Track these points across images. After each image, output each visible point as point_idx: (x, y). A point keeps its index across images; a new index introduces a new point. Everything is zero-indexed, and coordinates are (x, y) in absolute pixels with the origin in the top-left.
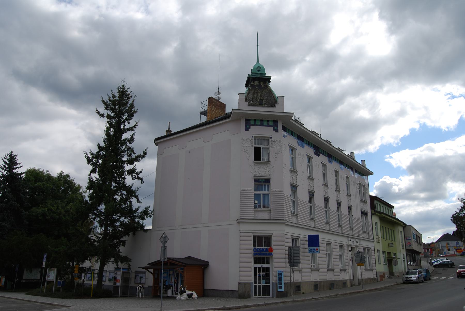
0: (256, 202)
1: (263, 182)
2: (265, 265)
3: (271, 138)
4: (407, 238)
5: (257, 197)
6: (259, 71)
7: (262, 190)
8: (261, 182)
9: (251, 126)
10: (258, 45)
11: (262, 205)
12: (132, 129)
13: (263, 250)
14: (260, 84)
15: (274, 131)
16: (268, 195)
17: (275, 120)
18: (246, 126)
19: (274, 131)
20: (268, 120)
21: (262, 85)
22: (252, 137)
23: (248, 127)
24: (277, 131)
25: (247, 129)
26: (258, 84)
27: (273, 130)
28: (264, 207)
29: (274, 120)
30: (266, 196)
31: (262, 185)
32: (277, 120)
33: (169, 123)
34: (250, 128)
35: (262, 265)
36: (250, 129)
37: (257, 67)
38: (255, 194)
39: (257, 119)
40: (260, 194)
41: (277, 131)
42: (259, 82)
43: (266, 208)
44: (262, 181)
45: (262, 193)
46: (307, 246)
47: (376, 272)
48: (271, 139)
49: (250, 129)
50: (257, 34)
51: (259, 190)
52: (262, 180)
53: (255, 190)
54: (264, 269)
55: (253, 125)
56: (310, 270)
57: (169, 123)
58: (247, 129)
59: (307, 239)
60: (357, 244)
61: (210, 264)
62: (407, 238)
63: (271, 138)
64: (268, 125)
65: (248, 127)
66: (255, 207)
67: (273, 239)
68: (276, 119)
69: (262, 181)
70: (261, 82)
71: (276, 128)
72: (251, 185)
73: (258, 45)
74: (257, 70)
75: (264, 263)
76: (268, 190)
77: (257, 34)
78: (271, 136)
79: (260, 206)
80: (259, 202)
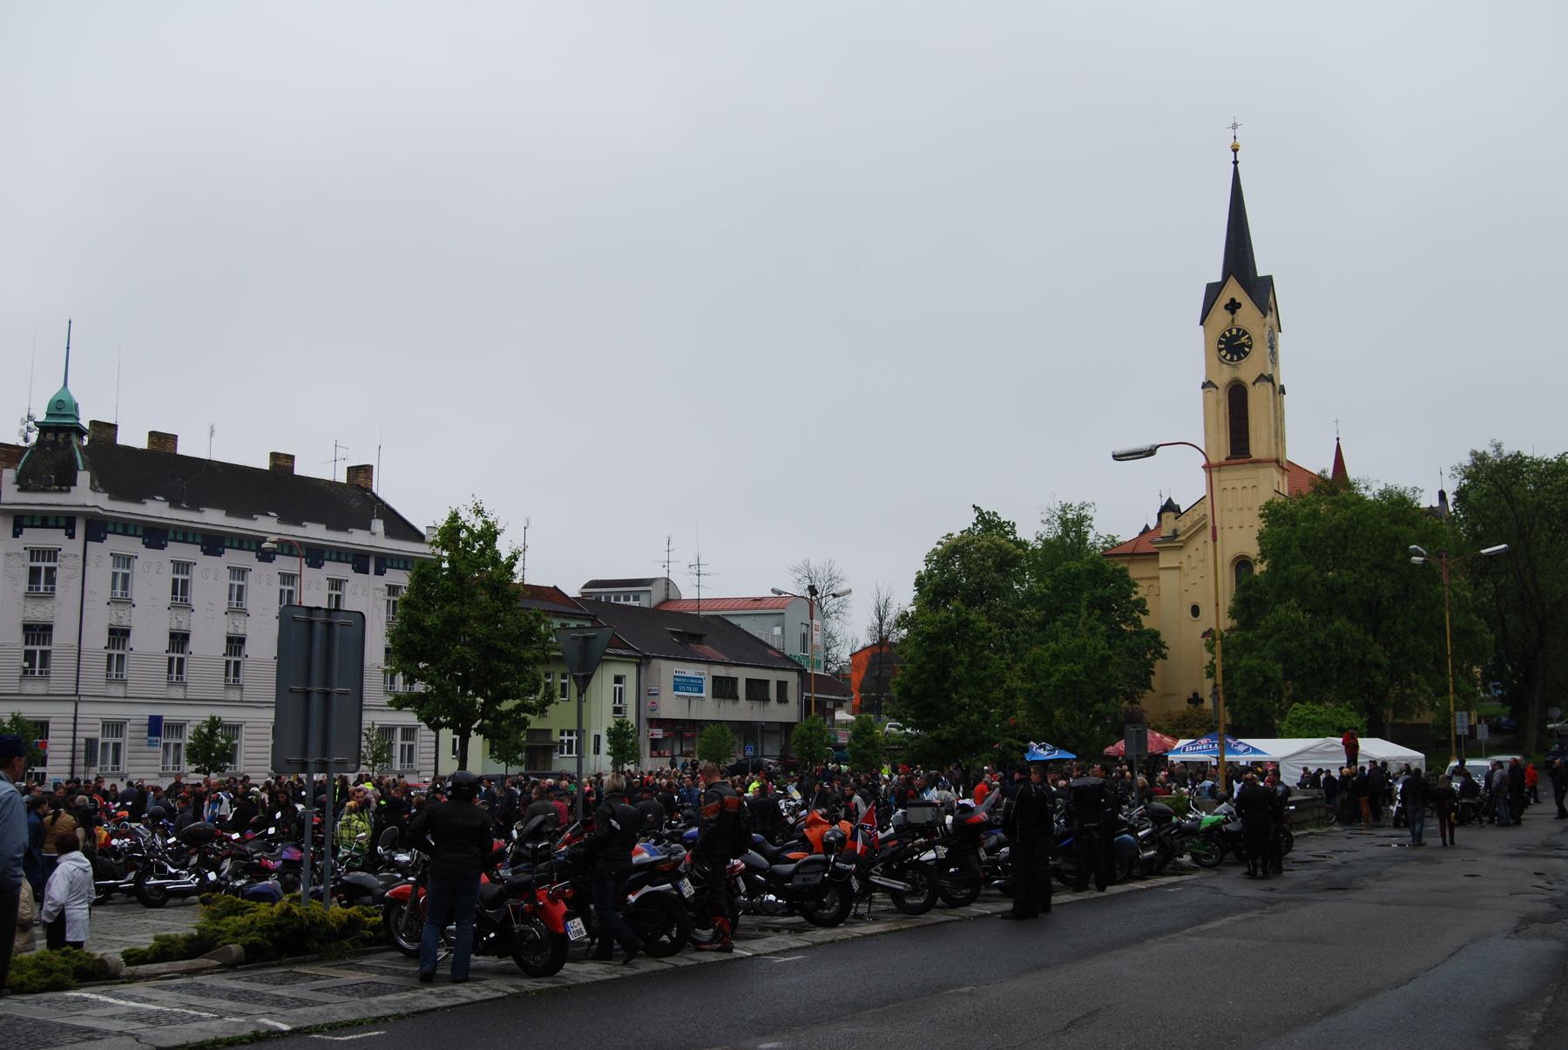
0: (26, 665)
1: (40, 630)
4: (651, 690)
5: (29, 656)
6: (60, 409)
7: (38, 644)
8: (36, 630)
10: (68, 348)
11: (37, 669)
16: (50, 651)
21: (60, 440)
22: (25, 549)
24: (72, 536)
25: (16, 535)
26: (53, 438)
28: (41, 672)
30: (45, 655)
31: (39, 635)
34: (21, 533)
38: (26, 651)
41: (72, 536)
43: (45, 674)
45: (38, 648)
46: (146, 734)
50: (70, 322)
51: (33, 644)
52: (38, 625)
53: (27, 643)
56: (156, 776)
58: (16, 535)
59: (147, 722)
62: (651, 690)
64: (57, 527)
66: (25, 672)
67: (51, 726)
71: (70, 531)
72: (18, 637)
73: (68, 348)
76: (50, 644)
77: (70, 322)
78: (60, 547)
79: (33, 672)
80: (32, 665)
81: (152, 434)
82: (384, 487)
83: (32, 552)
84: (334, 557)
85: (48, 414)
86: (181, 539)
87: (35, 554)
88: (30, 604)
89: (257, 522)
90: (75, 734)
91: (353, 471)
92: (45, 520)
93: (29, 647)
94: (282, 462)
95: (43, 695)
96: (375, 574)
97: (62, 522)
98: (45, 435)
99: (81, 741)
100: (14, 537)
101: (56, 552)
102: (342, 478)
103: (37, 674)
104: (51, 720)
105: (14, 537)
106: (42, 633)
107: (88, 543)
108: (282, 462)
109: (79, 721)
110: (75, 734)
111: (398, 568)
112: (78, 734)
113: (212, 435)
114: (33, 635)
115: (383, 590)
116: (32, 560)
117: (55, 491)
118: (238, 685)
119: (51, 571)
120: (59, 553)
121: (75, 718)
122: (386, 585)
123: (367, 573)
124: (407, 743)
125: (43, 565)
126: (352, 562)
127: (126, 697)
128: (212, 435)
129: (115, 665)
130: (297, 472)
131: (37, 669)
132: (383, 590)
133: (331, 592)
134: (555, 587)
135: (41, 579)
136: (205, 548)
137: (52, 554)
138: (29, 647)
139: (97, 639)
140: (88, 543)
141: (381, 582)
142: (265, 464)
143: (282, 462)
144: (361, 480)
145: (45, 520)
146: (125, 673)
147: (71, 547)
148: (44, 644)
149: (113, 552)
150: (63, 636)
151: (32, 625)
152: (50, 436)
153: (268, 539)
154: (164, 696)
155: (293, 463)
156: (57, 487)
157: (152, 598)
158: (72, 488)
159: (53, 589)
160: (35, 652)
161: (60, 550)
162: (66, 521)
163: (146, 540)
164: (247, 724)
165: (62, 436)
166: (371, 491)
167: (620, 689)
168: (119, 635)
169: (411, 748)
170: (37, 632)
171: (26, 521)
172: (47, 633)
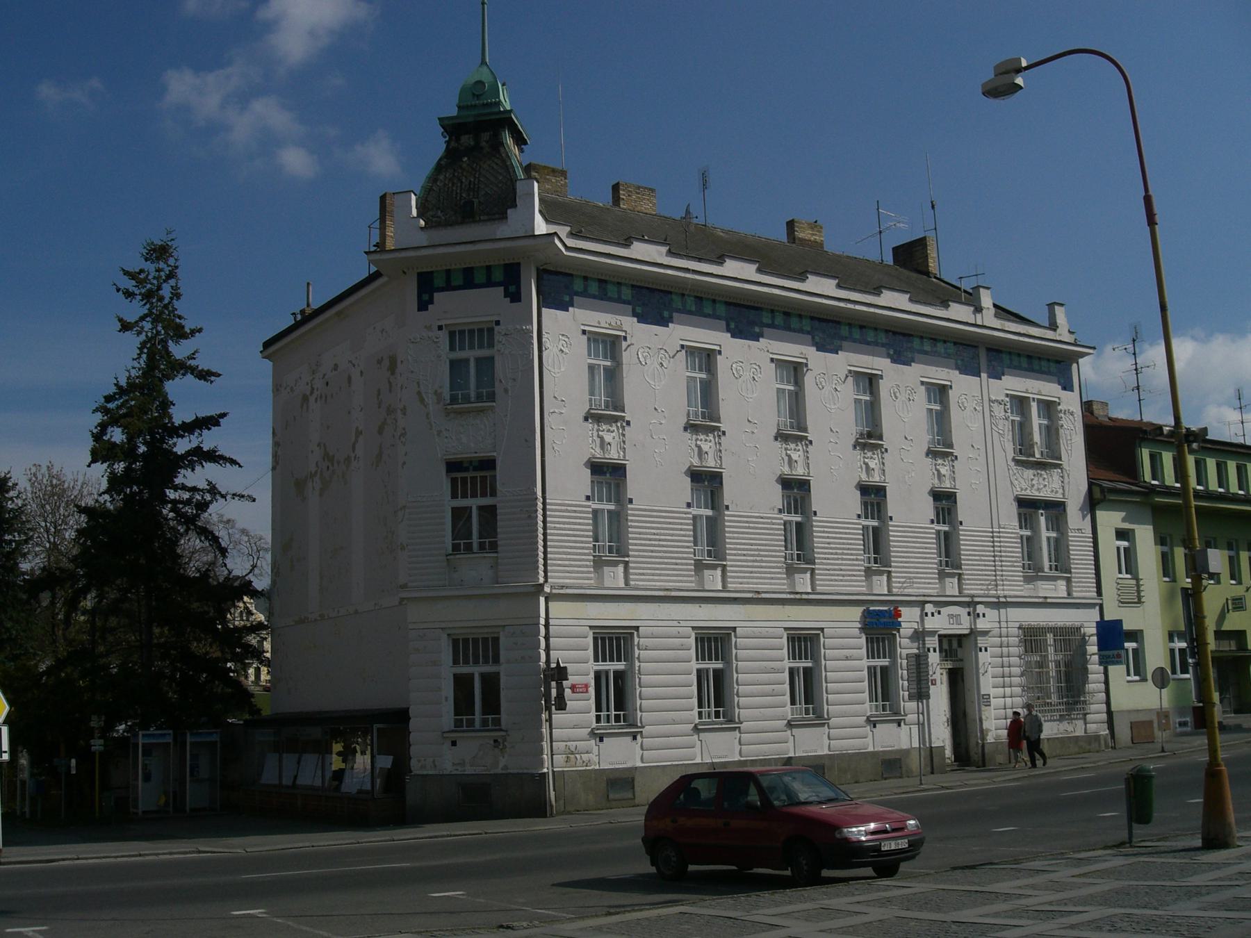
3: (498, 323)
6: (478, 97)
8: (466, 470)
9: (435, 294)
15: (509, 299)
17: (512, 261)
19: (509, 299)
20: (487, 266)
23: (425, 297)
25: (423, 306)
27: (505, 296)
29: (507, 262)
32: (516, 261)
34: (431, 301)
36: (432, 303)
37: (474, 81)
39: (453, 267)
44: (471, 468)
47: (1110, 713)
48: (497, 328)
49: (432, 303)
51: (464, 496)
52: (471, 462)
53: (454, 496)
55: (442, 290)
58: (423, 306)
63: (498, 323)
64: (489, 284)
65: (425, 297)
68: (513, 259)
69: (471, 468)
70: (482, 134)
71: (512, 289)
74: (474, 94)
83: (452, 335)
85: (459, 107)
86: (693, 309)
87: (457, 337)
92: (468, 279)
93: (461, 503)
97: (498, 275)
98: (458, 140)
100: (420, 309)
101: (491, 330)
105: (420, 309)
106: (479, 474)
113: (705, 186)
120: (497, 328)
122: (1007, 395)
125: (471, 354)
128: (705, 186)
136: (733, 325)
137: (485, 334)
138: (461, 503)
149: (587, 328)
151: (461, 463)
152: (467, 140)
165: (485, 136)
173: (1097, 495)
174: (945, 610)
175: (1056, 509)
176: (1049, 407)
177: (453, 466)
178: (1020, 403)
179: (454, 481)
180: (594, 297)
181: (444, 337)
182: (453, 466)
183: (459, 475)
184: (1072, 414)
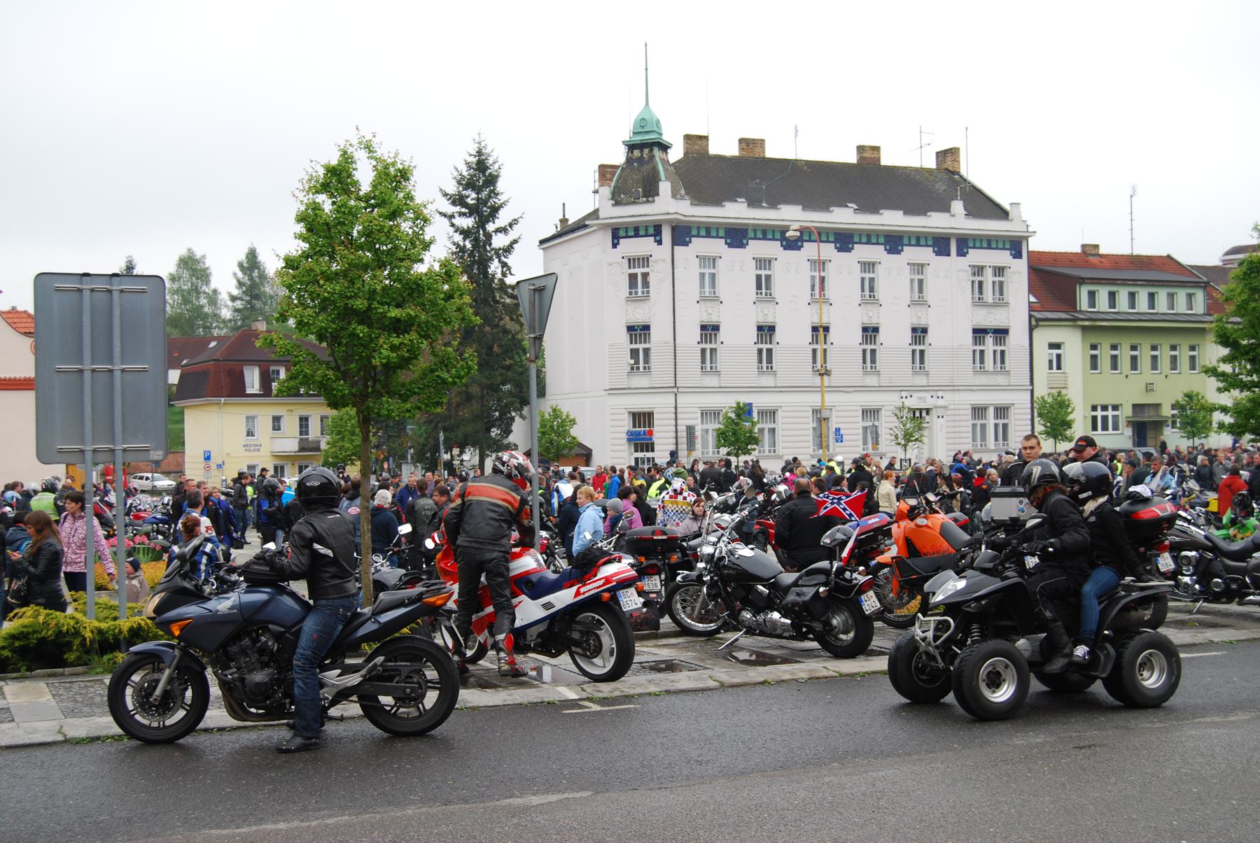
1: (641, 330)
2: (649, 455)
5: (634, 353)
12: (502, 230)
13: (639, 433)
14: (642, 155)
18: (613, 241)
23: (616, 241)
24: (660, 243)
25: (615, 246)
28: (645, 368)
30: (647, 352)
31: (640, 335)
33: (564, 204)
35: (645, 453)
38: (631, 350)
40: (638, 349)
41: (660, 243)
42: (642, 152)
45: (641, 346)
52: (638, 326)
54: (649, 459)
57: (564, 204)
58: (615, 246)
60: (940, 402)
61: (593, 453)
63: (651, 256)
65: (616, 241)
66: (632, 369)
67: (656, 416)
71: (658, 238)
72: (625, 336)
75: (647, 451)
79: (638, 368)
80: (637, 362)
81: (741, 141)
82: (973, 170)
84: (913, 242)
86: (761, 236)
87: (632, 261)
88: (632, 306)
89: (781, 211)
90: (676, 422)
91: (943, 155)
92: (636, 231)
94: (869, 155)
95: (649, 388)
96: (958, 256)
97: (651, 231)
98: (632, 152)
99: (682, 429)
101: (648, 258)
102: (931, 163)
103: (641, 370)
104: (655, 411)
106: (643, 332)
107: (675, 247)
108: (868, 155)
109: (679, 410)
110: (676, 422)
111: (982, 248)
112: (679, 422)
113: (796, 135)
114: (636, 335)
115: (966, 271)
116: (630, 268)
117: (643, 203)
118: (715, 371)
119: (645, 275)
120: (650, 259)
121: (676, 408)
123: (949, 255)
124: (1001, 422)
125: (639, 271)
126: (933, 246)
127: (720, 387)
128: (796, 135)
129: (708, 358)
130: (883, 162)
131: (641, 365)
132: (966, 271)
133: (913, 277)
134: (1169, 256)
135: (638, 283)
137: (645, 261)
139: (690, 336)
140: (675, 247)
141: (964, 263)
142: (852, 158)
143: (869, 155)
144: (949, 164)
145: (636, 231)
146: (718, 365)
147: (660, 253)
148: (645, 342)
150: (660, 336)
151: (634, 326)
152: (637, 153)
153: (791, 228)
154: (756, 385)
155: (879, 154)
156: (644, 199)
157: (738, 294)
158: (656, 198)
159: (648, 292)
160: (638, 349)
161: (651, 256)
162: (655, 231)
163: (729, 241)
164: (783, 409)
165: (646, 151)
166: (958, 173)
167: (1059, 356)
168: (709, 330)
169: (1005, 426)
170: (639, 331)
171: (622, 233)
172: (647, 332)
173: (1034, 323)
174: (915, 395)
175: (1001, 333)
176: (999, 271)
177: (630, 329)
178: (979, 270)
179: (631, 335)
180: (703, 237)
181: (625, 262)
182: (630, 329)
183: (633, 333)
184: (1020, 273)
